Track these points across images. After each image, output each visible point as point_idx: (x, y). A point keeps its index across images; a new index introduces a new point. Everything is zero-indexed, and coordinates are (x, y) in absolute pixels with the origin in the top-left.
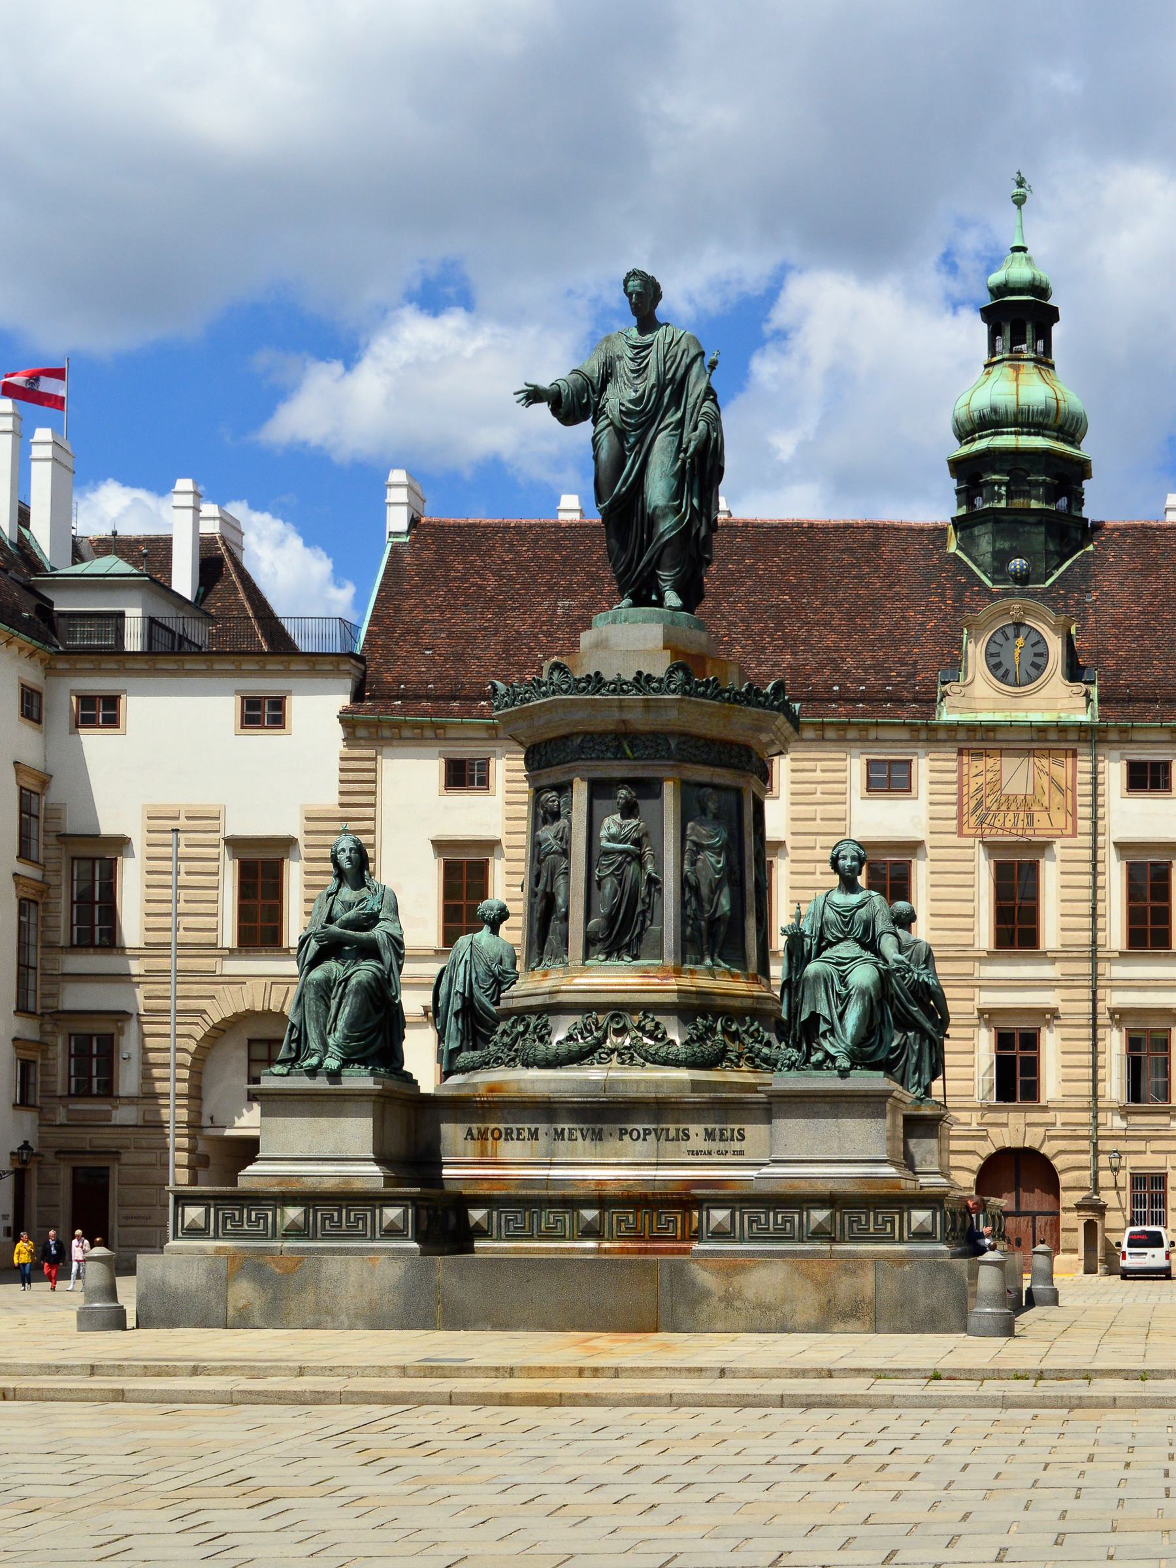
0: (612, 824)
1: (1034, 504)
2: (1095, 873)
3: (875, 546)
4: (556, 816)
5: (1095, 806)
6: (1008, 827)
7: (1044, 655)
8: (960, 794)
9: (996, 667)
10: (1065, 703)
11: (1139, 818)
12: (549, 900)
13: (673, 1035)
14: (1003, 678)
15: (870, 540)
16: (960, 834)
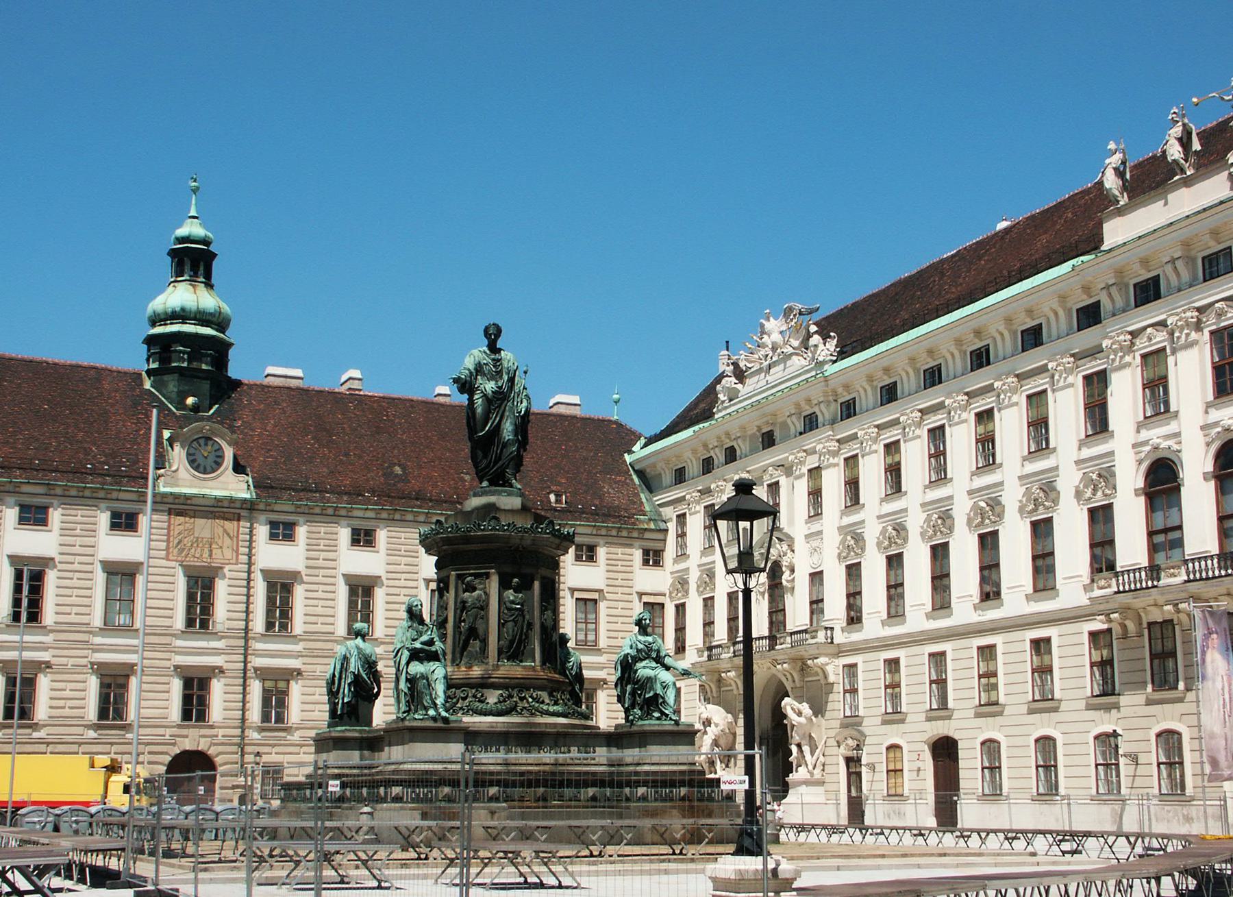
0: (510, 594)
1: (204, 367)
2: (249, 587)
3: (99, 380)
4: (474, 589)
5: (250, 548)
6: (199, 558)
7: (222, 457)
8: (168, 535)
9: (193, 462)
10: (234, 486)
11: (274, 555)
12: (473, 633)
13: (547, 701)
14: (197, 469)
15: (96, 376)
16: (168, 559)
